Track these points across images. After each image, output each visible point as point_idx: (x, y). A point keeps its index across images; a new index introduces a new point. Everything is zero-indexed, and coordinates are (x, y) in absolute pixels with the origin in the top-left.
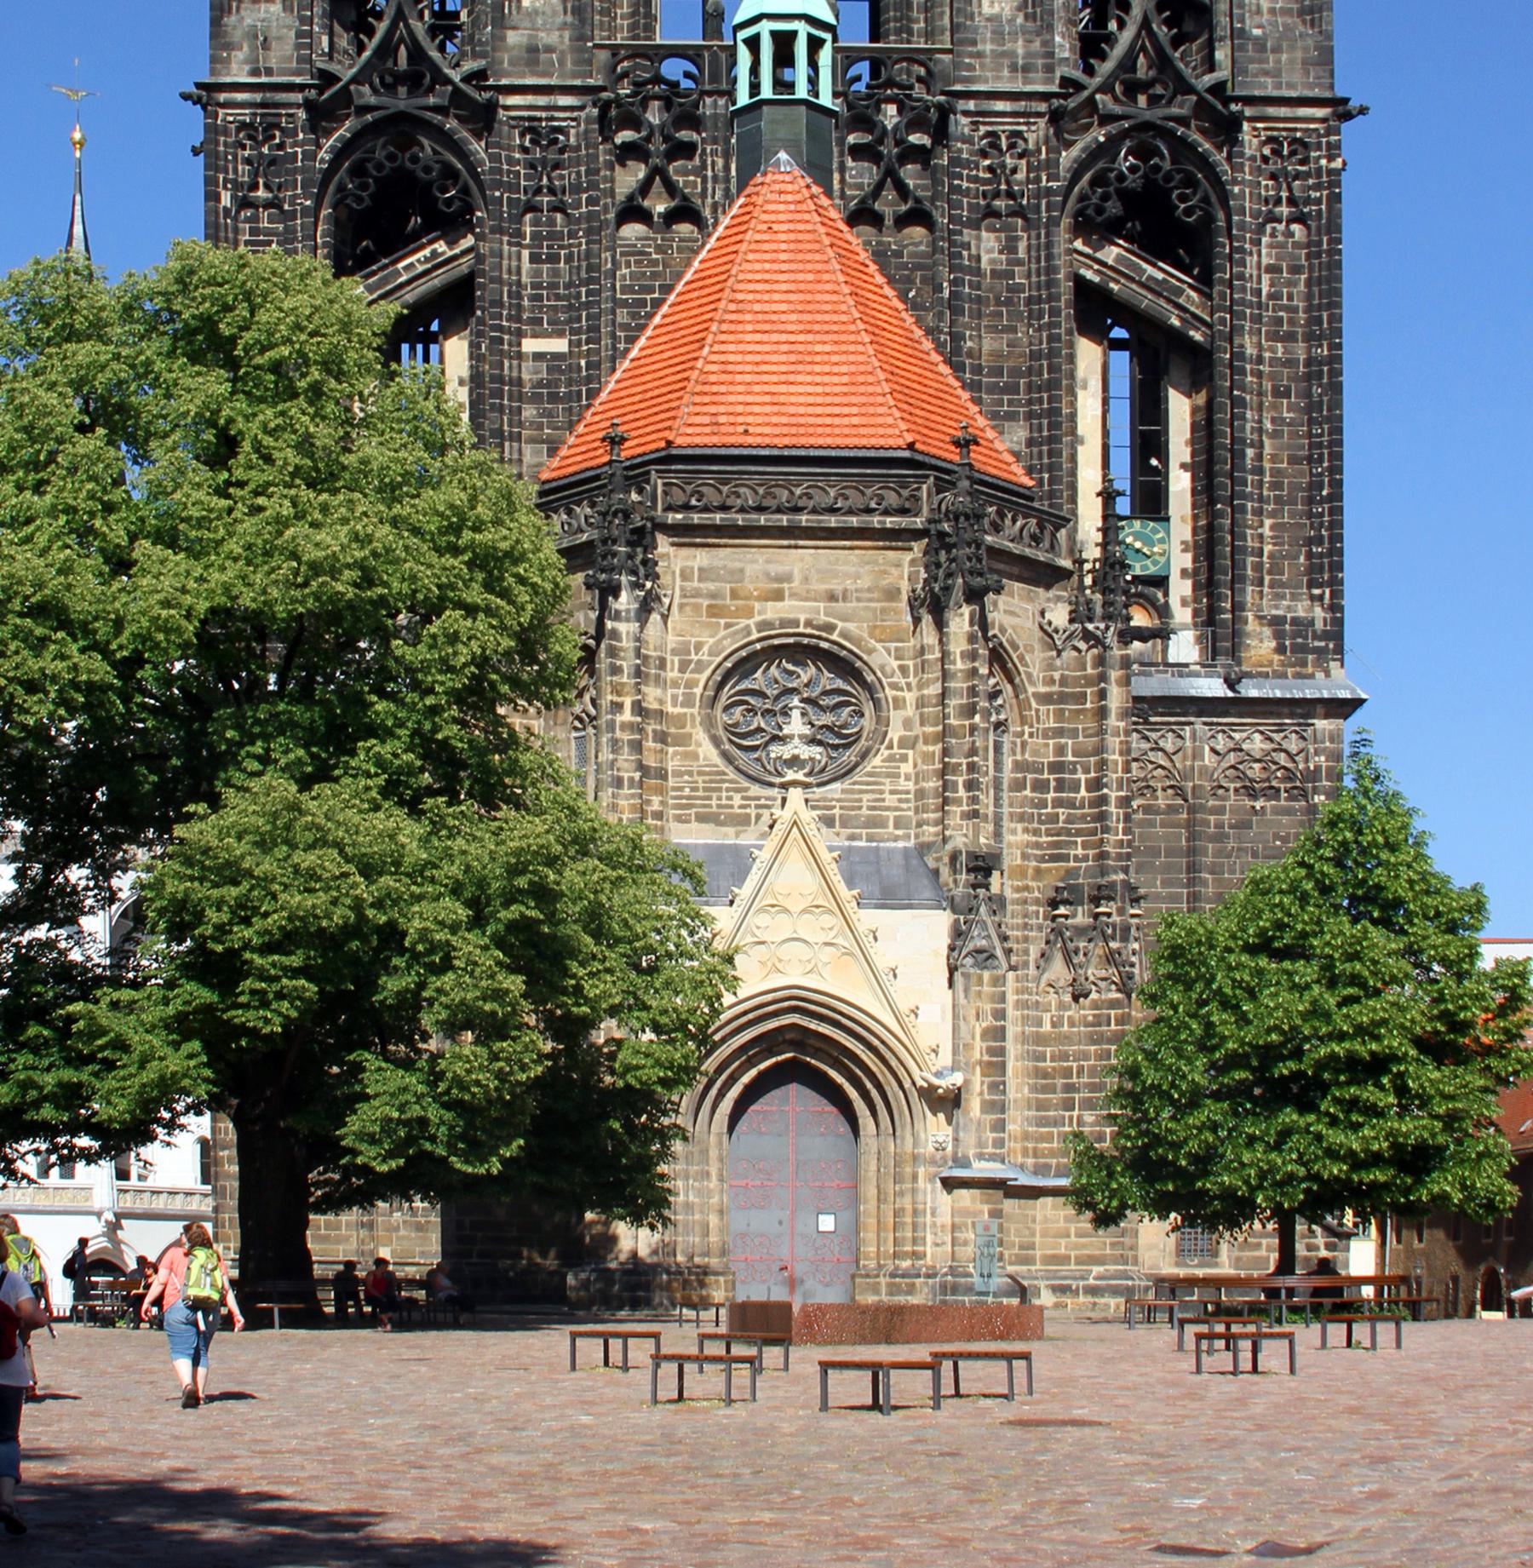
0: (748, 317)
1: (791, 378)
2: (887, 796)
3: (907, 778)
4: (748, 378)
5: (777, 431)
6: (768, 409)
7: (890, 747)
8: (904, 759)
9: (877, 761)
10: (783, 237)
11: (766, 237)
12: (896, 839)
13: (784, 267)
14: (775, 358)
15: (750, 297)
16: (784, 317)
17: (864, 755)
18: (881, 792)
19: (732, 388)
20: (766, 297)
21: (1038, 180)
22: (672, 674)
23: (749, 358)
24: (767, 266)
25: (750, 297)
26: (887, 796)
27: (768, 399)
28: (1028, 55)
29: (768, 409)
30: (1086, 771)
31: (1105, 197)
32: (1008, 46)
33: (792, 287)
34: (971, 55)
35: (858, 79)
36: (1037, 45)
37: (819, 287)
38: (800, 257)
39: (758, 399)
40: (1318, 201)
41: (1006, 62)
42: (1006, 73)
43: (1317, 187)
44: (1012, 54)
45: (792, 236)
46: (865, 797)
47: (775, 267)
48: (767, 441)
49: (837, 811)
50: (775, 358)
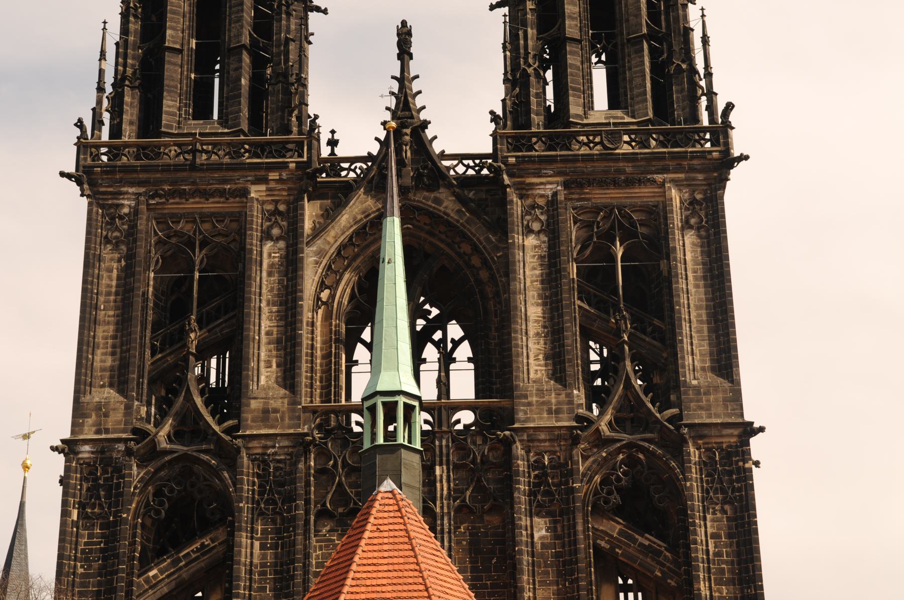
0: (363, 589)
10: (386, 534)
11: (376, 534)
13: (386, 554)
15: (364, 575)
16: (384, 589)
20: (374, 575)
21: (567, 483)
24: (376, 555)
25: (364, 575)
28: (558, 403)
31: (610, 493)
32: (546, 398)
33: (391, 567)
34: (524, 405)
35: (458, 421)
36: (563, 397)
37: (407, 567)
38: (396, 547)
40: (740, 489)
41: (545, 408)
42: (545, 415)
43: (738, 480)
44: (549, 403)
45: (392, 534)
47: (381, 554)
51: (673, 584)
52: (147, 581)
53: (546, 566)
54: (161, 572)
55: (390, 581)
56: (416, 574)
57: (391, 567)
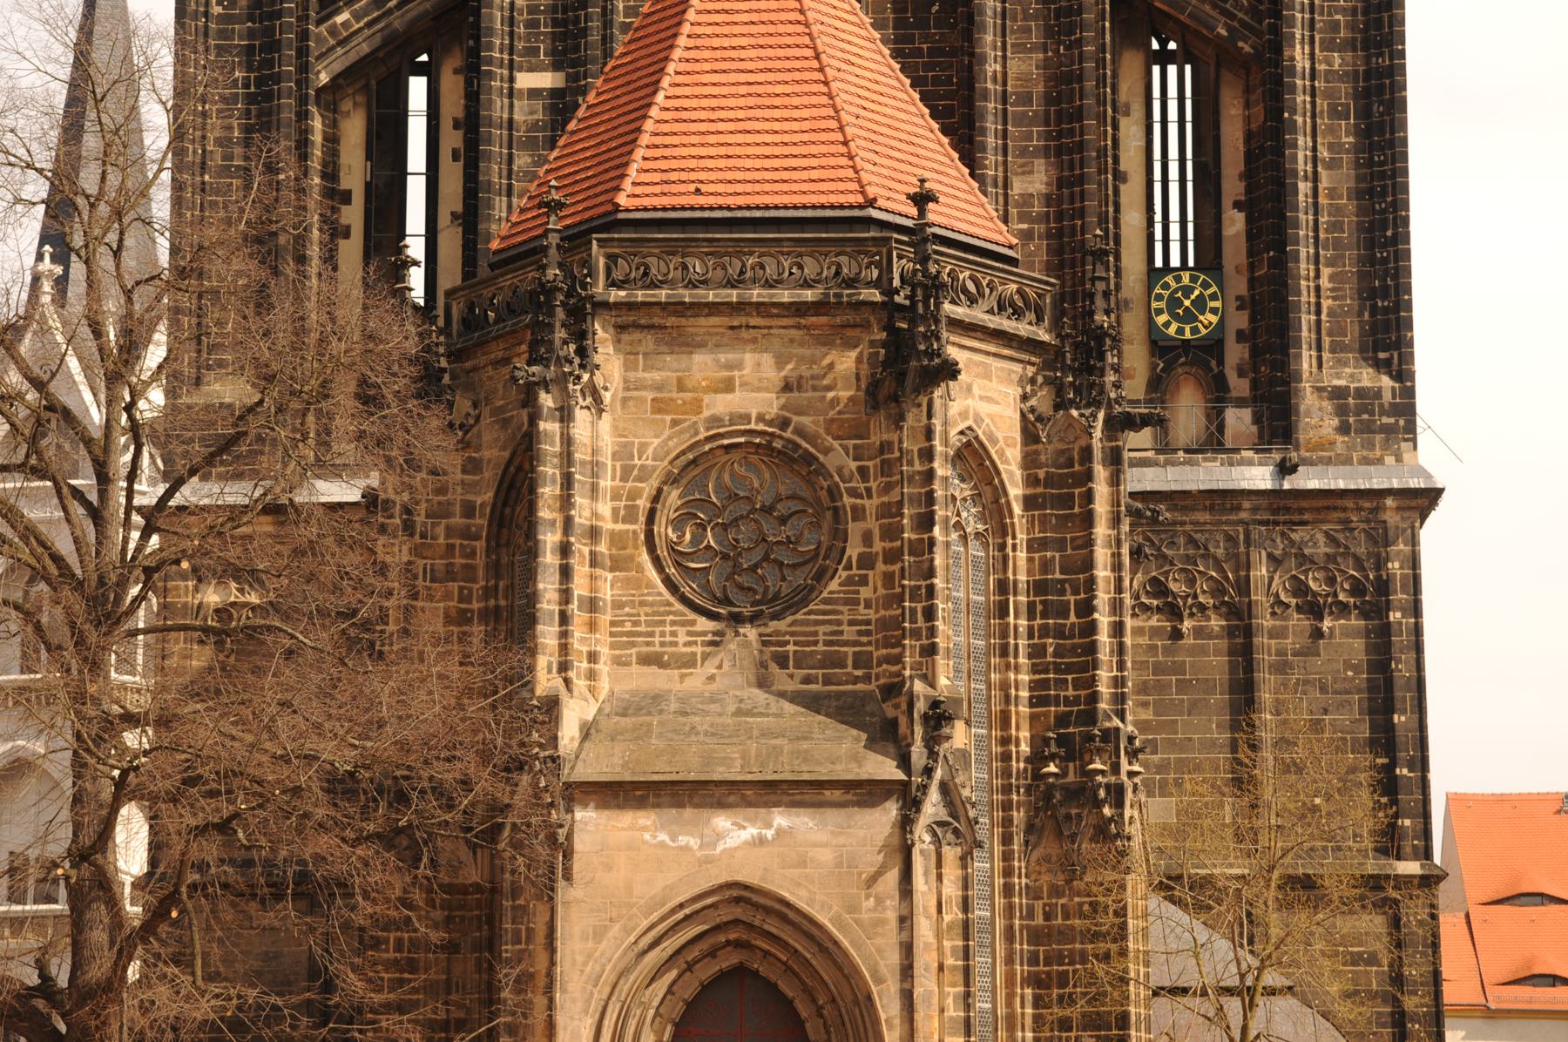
0: (707, 54)
1: (749, 126)
2: (845, 628)
3: (868, 605)
4: (703, 127)
5: (731, 188)
6: (722, 163)
7: (849, 567)
8: (864, 581)
9: (834, 585)
12: (856, 680)
14: (732, 102)
15: (709, 30)
17: (822, 576)
18: (839, 623)
19: (685, 140)
20: (726, 30)
22: (606, 483)
23: (705, 103)
25: (709, 30)
26: (845, 628)
27: (723, 151)
29: (722, 163)
33: (755, 17)
37: (784, 16)
39: (713, 151)
46: (822, 629)
48: (720, 201)
49: (791, 648)
50: (732, 102)
51: (1247, 49)
52: (333, 31)
53: (1026, 17)
54: (357, 16)
55: (753, 41)
56: (800, 29)
57: (755, 17)
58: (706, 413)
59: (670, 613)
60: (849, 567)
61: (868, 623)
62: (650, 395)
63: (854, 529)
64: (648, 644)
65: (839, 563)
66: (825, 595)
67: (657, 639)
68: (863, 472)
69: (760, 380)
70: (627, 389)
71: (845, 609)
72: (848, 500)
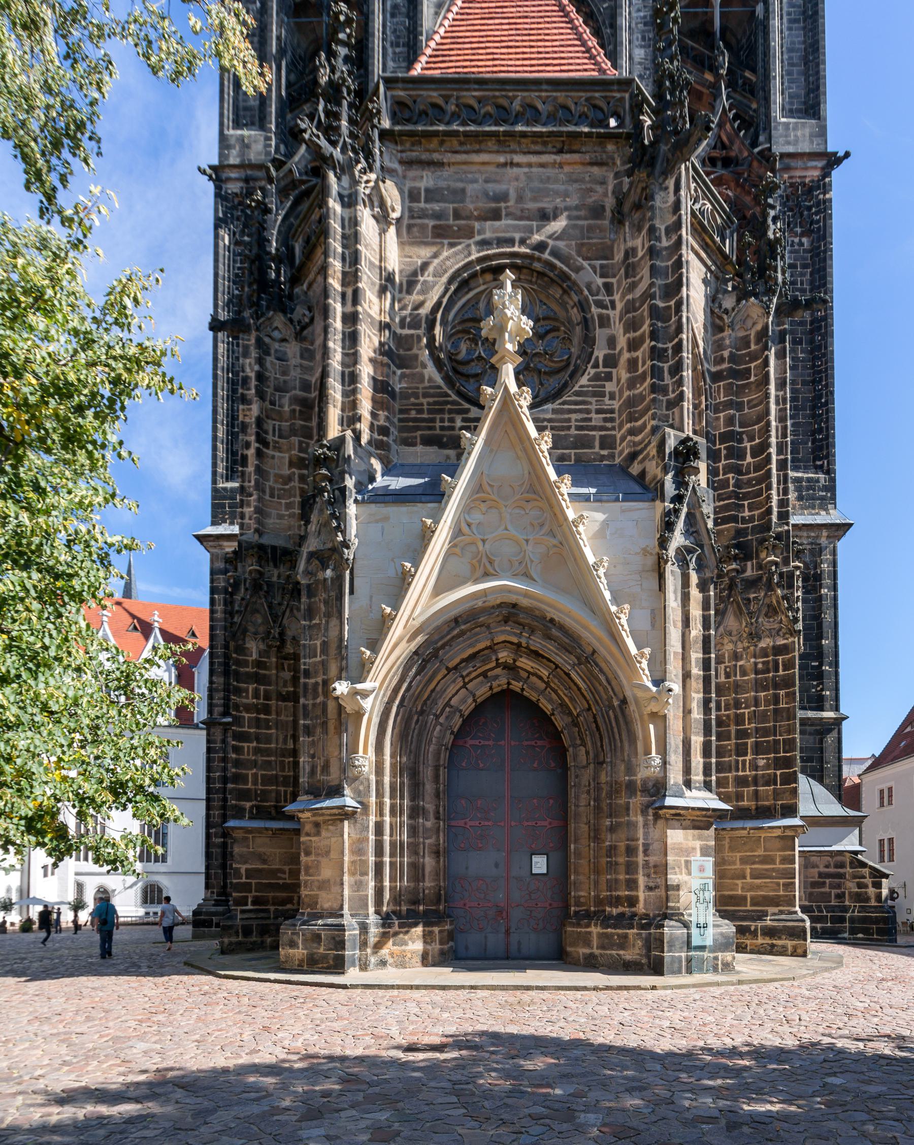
2: (593, 415)
7: (596, 366)
8: (609, 377)
9: (584, 380)
18: (588, 411)
26: (593, 415)
30: (751, 439)
46: (574, 416)
58: (478, 238)
59: (448, 403)
60: (596, 366)
61: (612, 411)
62: (431, 223)
63: (601, 334)
64: (430, 428)
65: (589, 362)
66: (576, 388)
67: (438, 424)
68: (608, 288)
69: (522, 211)
70: (412, 217)
71: (593, 400)
72: (595, 310)
